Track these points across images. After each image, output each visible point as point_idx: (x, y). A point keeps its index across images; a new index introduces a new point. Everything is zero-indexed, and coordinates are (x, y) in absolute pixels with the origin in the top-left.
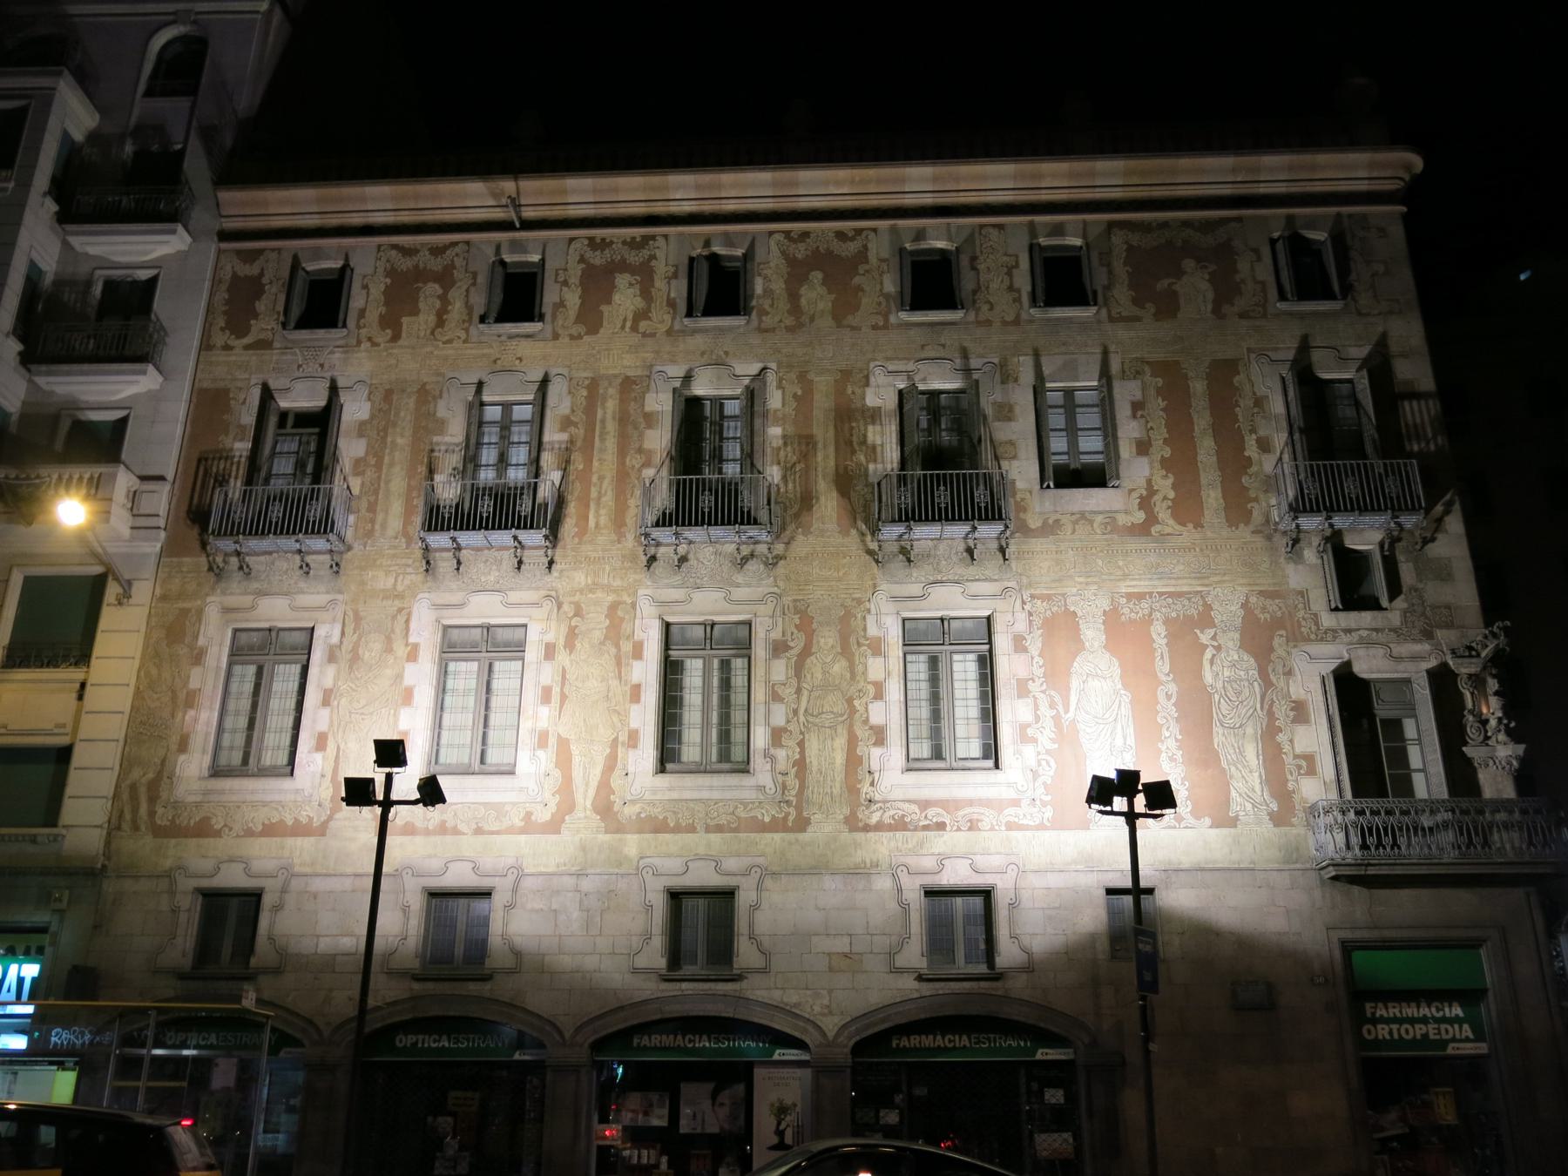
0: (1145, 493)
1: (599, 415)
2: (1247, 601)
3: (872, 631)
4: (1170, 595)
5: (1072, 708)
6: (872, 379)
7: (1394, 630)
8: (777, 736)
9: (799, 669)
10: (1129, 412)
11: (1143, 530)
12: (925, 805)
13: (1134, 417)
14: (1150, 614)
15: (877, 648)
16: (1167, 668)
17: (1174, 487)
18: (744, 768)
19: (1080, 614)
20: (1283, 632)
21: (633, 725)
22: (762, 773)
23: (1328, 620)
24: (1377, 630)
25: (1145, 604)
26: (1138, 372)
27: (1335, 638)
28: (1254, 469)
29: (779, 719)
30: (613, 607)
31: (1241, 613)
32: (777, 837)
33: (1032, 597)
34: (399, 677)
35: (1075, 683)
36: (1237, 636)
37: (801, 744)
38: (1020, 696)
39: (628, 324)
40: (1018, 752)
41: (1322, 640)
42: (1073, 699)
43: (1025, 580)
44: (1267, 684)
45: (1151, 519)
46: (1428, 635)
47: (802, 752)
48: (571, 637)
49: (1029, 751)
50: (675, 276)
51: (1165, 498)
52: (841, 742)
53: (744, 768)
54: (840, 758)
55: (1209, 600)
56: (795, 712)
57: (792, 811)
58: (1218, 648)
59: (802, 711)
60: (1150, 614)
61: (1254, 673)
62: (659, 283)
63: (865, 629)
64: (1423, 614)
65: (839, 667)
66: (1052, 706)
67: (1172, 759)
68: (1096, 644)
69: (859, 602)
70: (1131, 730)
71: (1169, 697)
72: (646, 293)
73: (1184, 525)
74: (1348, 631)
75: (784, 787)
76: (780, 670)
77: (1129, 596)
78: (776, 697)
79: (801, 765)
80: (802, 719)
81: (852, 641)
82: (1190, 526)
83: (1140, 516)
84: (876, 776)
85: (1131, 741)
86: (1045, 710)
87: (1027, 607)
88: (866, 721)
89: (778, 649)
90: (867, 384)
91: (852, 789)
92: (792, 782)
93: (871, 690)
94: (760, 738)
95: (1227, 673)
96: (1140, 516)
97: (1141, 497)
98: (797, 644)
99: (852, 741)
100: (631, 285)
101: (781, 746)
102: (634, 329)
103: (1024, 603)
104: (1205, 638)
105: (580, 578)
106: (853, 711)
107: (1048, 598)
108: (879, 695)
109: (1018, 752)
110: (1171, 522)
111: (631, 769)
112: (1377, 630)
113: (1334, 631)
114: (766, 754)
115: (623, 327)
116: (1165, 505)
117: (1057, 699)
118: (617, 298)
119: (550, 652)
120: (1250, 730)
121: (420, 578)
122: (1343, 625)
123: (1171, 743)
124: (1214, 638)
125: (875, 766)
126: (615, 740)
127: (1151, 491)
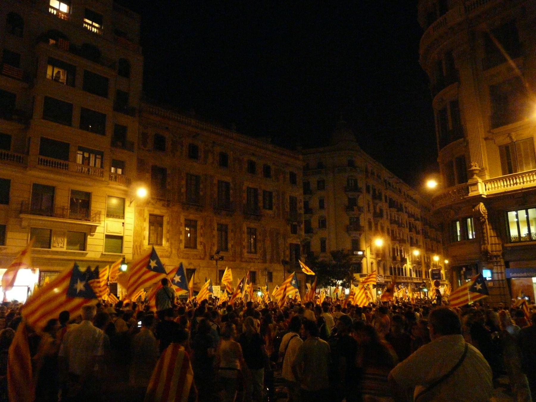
11: (273, 218)
12: (249, 258)
15: (244, 233)
46: (300, 239)
48: (205, 225)
54: (239, 250)
76: (232, 234)
89: (232, 231)
94: (230, 246)
119: (202, 228)
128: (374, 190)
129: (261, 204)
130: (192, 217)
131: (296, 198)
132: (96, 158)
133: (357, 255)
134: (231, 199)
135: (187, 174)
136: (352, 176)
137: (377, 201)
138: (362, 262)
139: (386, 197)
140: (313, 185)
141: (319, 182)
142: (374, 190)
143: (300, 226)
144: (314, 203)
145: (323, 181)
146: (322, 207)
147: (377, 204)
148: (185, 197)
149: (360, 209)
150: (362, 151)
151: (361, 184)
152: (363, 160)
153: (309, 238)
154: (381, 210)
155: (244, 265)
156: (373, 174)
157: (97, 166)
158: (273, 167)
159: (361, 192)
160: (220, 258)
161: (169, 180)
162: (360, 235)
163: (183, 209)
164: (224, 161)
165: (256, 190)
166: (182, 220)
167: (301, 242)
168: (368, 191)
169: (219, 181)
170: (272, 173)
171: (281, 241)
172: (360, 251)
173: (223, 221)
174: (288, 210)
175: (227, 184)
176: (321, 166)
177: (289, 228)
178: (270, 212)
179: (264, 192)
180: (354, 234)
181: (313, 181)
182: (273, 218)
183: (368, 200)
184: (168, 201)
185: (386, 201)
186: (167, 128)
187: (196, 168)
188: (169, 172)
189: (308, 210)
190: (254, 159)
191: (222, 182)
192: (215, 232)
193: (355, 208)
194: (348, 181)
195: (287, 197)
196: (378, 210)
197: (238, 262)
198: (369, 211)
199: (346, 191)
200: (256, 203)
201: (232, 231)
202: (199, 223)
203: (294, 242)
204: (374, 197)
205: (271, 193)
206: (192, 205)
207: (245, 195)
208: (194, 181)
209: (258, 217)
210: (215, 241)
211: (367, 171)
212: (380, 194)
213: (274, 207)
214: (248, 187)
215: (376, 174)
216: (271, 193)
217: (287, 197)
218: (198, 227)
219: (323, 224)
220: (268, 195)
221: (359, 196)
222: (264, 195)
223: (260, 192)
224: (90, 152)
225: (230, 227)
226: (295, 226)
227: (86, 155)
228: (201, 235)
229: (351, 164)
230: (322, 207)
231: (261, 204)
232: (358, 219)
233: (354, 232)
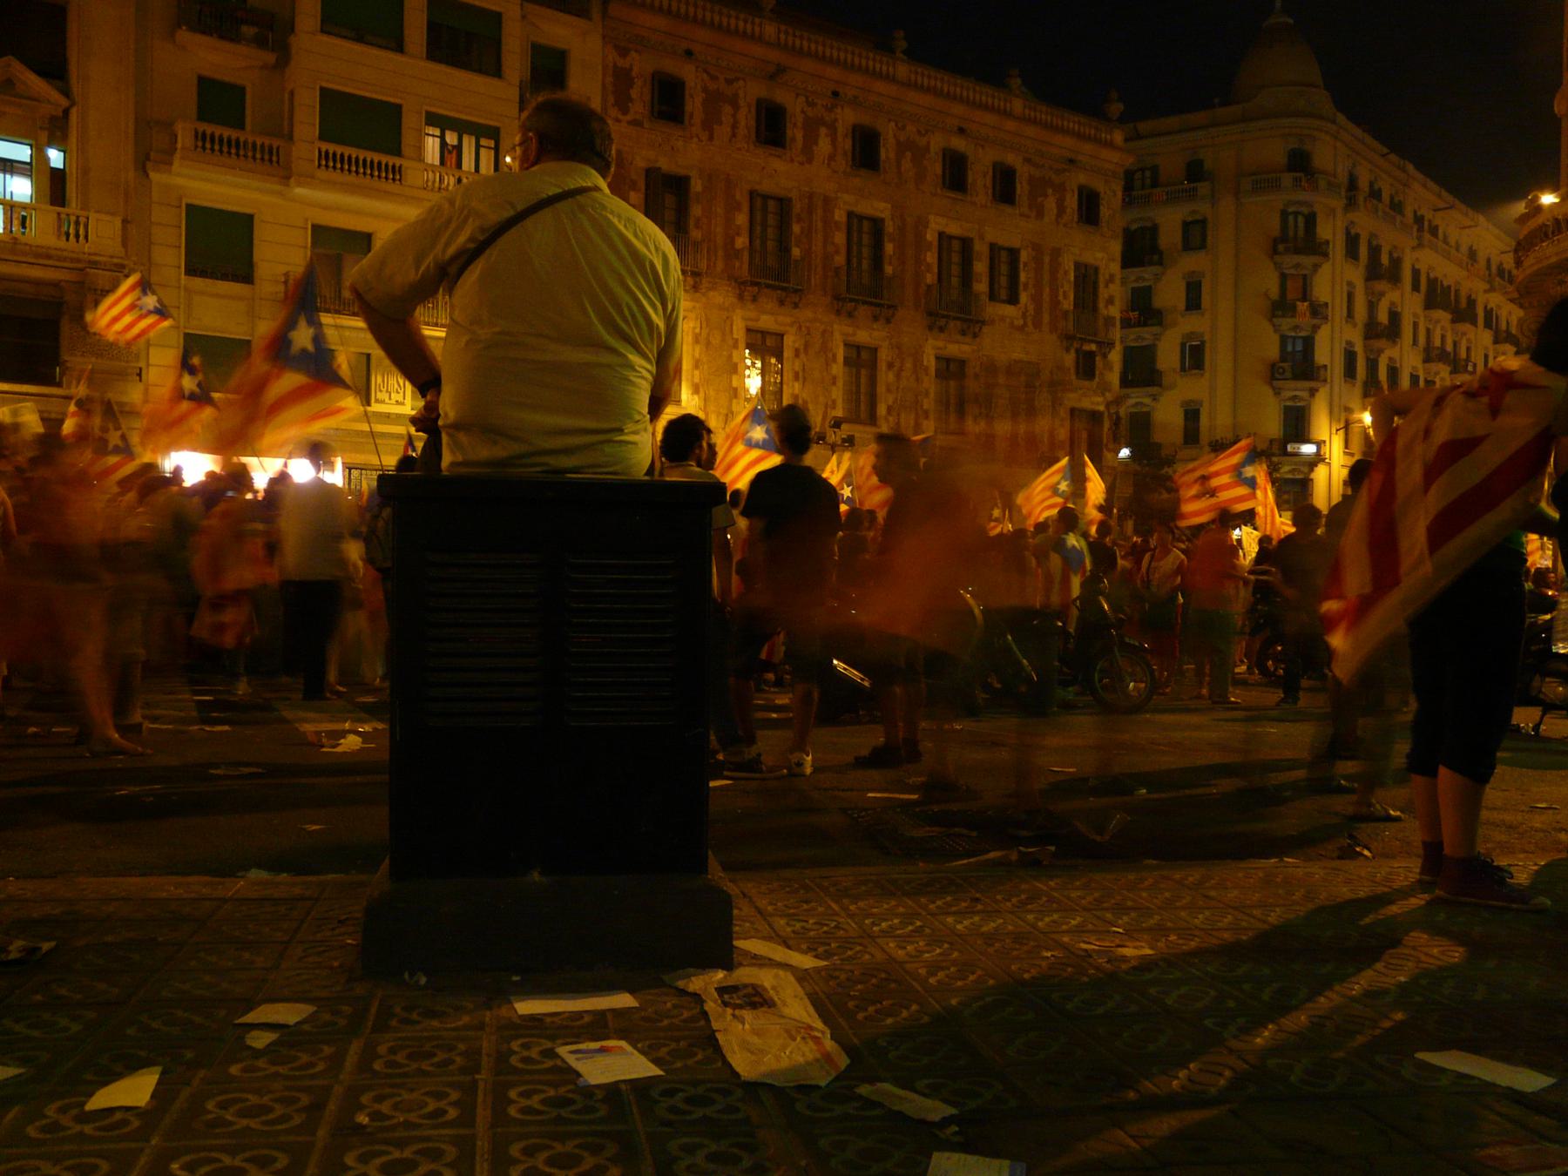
8: (889, 409)
9: (898, 376)
11: (1021, 329)
15: (926, 369)
30: (824, 331)
34: (730, 357)
45: (1025, 324)
48: (806, 346)
52: (913, 416)
54: (912, 423)
76: (891, 376)
94: (882, 410)
98: (897, 364)
105: (809, 314)
119: (797, 353)
121: (735, 300)
128: (1375, 251)
129: (981, 287)
130: (767, 322)
131: (1096, 269)
132: (478, 147)
133: (1297, 454)
134: (889, 270)
135: (752, 194)
136: (1300, 203)
137: (1381, 286)
138: (1313, 476)
139: (1416, 273)
140: (1170, 235)
141: (1186, 225)
142: (1375, 251)
143: (1105, 356)
144: (1169, 293)
145: (1203, 222)
146: (1194, 302)
147: (1382, 294)
148: (746, 266)
149: (1318, 311)
150: (1341, 118)
151: (1330, 231)
152: (1339, 148)
153: (1147, 400)
154: (1395, 317)
156: (1375, 194)
157: (483, 170)
158: (1023, 171)
159: (1326, 255)
160: (844, 441)
161: (696, 210)
162: (1313, 392)
163: (741, 297)
164: (865, 151)
165: (966, 243)
166: (739, 333)
167: (1108, 406)
168: (1352, 251)
169: (850, 215)
170: (1022, 188)
172: (1308, 441)
173: (863, 337)
174: (1068, 304)
175: (877, 224)
176: (1195, 172)
177: (1069, 359)
178: (1009, 310)
179: (994, 248)
180: (1295, 390)
181: (1170, 221)
182: (1021, 329)
183: (1350, 284)
184: (696, 274)
185: (1416, 288)
186: (689, 53)
187: (779, 173)
188: (697, 186)
189: (1143, 310)
190: (959, 143)
191: (861, 218)
192: (838, 369)
193: (1303, 307)
194: (1284, 220)
195: (1068, 263)
196: (1383, 317)
198: (1350, 315)
199: (1275, 252)
200: (967, 278)
201: (890, 366)
202: (790, 342)
204: (1374, 272)
205: (1013, 254)
206: (768, 286)
207: (931, 258)
208: (774, 212)
209: (972, 324)
210: (838, 393)
211: (1352, 185)
212: (1396, 263)
214: (941, 235)
215: (1386, 196)
216: (1013, 254)
217: (1068, 263)
218: (788, 354)
219: (1194, 357)
220: (1006, 259)
221: (1316, 267)
222: (992, 259)
223: (980, 248)
224: (462, 127)
225: (884, 355)
226: (1091, 354)
227: (451, 138)
228: (796, 377)
229: (1300, 163)
230: (1194, 302)
231: (981, 287)
232: (1309, 343)
233: (1291, 384)
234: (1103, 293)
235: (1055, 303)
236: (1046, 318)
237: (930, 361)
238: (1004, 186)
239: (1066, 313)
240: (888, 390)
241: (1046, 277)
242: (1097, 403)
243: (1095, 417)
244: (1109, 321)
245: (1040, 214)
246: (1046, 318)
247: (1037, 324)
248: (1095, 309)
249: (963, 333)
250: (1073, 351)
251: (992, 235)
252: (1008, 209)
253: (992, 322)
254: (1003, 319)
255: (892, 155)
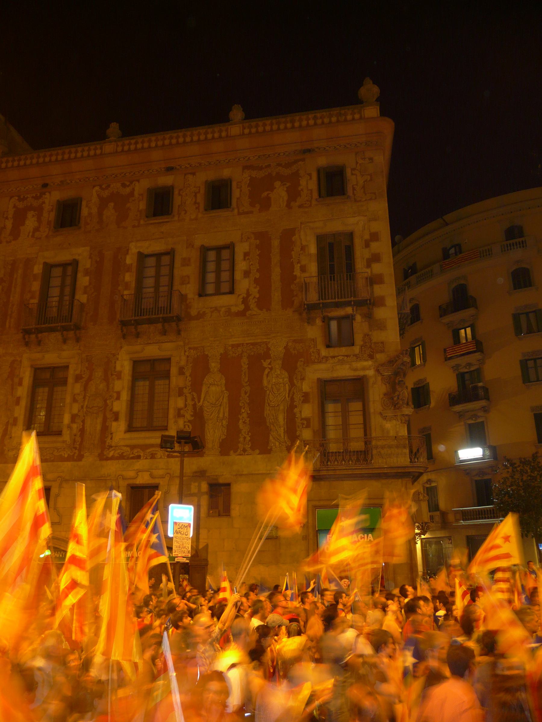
0: (245, 296)
1: (15, 276)
2: (287, 345)
3: (118, 368)
4: (252, 344)
5: (202, 400)
6: (130, 251)
7: (355, 355)
8: (73, 418)
10: (242, 257)
11: (242, 314)
13: (244, 259)
14: (242, 354)
16: (246, 380)
17: (259, 292)
18: (59, 433)
19: (210, 355)
20: (302, 359)
21: (16, 415)
22: (66, 436)
23: (324, 352)
24: (347, 356)
25: (240, 349)
26: (249, 238)
27: (327, 360)
28: (298, 280)
29: (75, 411)
31: (284, 351)
32: (69, 464)
33: (190, 348)
35: (204, 389)
36: (280, 362)
37: (83, 421)
38: (179, 396)
39: (31, 234)
40: (176, 422)
41: (320, 362)
42: (203, 396)
43: (187, 341)
44: (292, 384)
45: (247, 308)
46: (371, 357)
47: (83, 426)
49: (181, 422)
50: (52, 210)
51: (254, 297)
52: (100, 420)
53: (59, 433)
54: (99, 427)
55: (269, 346)
56: (82, 407)
57: (77, 451)
58: (271, 369)
59: (85, 406)
60: (242, 354)
61: (286, 380)
62: (45, 214)
63: (115, 368)
64: (370, 347)
65: (102, 386)
66: (193, 399)
67: (244, 422)
68: (216, 370)
69: (114, 355)
70: (227, 409)
71: (246, 393)
72: (39, 220)
73: (261, 310)
74: (333, 357)
75: (75, 441)
76: (78, 388)
77: (233, 346)
78: (75, 400)
79: (82, 431)
80: (85, 410)
81: (110, 374)
82: (264, 310)
83: (242, 307)
84: (114, 435)
85: (227, 415)
86: (190, 402)
87: (187, 354)
88: (111, 410)
89: (78, 378)
90: (127, 253)
91: (102, 441)
92: (78, 439)
93: (115, 395)
94: (67, 419)
95: (274, 381)
96: (242, 307)
97: (243, 298)
99: (105, 420)
100: (33, 216)
101: (75, 422)
102: (33, 236)
103: (185, 351)
104: (265, 364)
106: (106, 405)
107: (195, 349)
108: (118, 398)
109: (176, 422)
110: (256, 309)
111: (13, 435)
112: (347, 356)
113: (327, 357)
114: (69, 427)
115: (28, 236)
116: (254, 301)
117: (195, 395)
118: (27, 222)
120: (282, 407)
122: (331, 354)
123: (245, 415)
124: (270, 364)
125: (113, 429)
126: (8, 421)
127: (248, 294)
134: (82, 297)
143: (369, 316)
155: (111, 468)
171: (275, 379)
177: (314, 332)
178: (224, 300)
182: (242, 314)
197: (89, 459)
203: (344, 372)
213: (244, 285)
216: (231, 247)
222: (204, 262)
226: (350, 318)
234: (361, 254)
235: (288, 277)
236: (276, 296)
237: (124, 365)
238: (218, 196)
239: (306, 287)
240: (75, 400)
241: (275, 259)
242: (366, 368)
243: (357, 388)
244: (374, 280)
245: (266, 205)
246: (276, 296)
247: (264, 303)
248: (350, 267)
249: (164, 333)
250: (319, 322)
251: (201, 240)
252: (223, 213)
253: (200, 316)
254: (216, 309)
255: (94, 210)
